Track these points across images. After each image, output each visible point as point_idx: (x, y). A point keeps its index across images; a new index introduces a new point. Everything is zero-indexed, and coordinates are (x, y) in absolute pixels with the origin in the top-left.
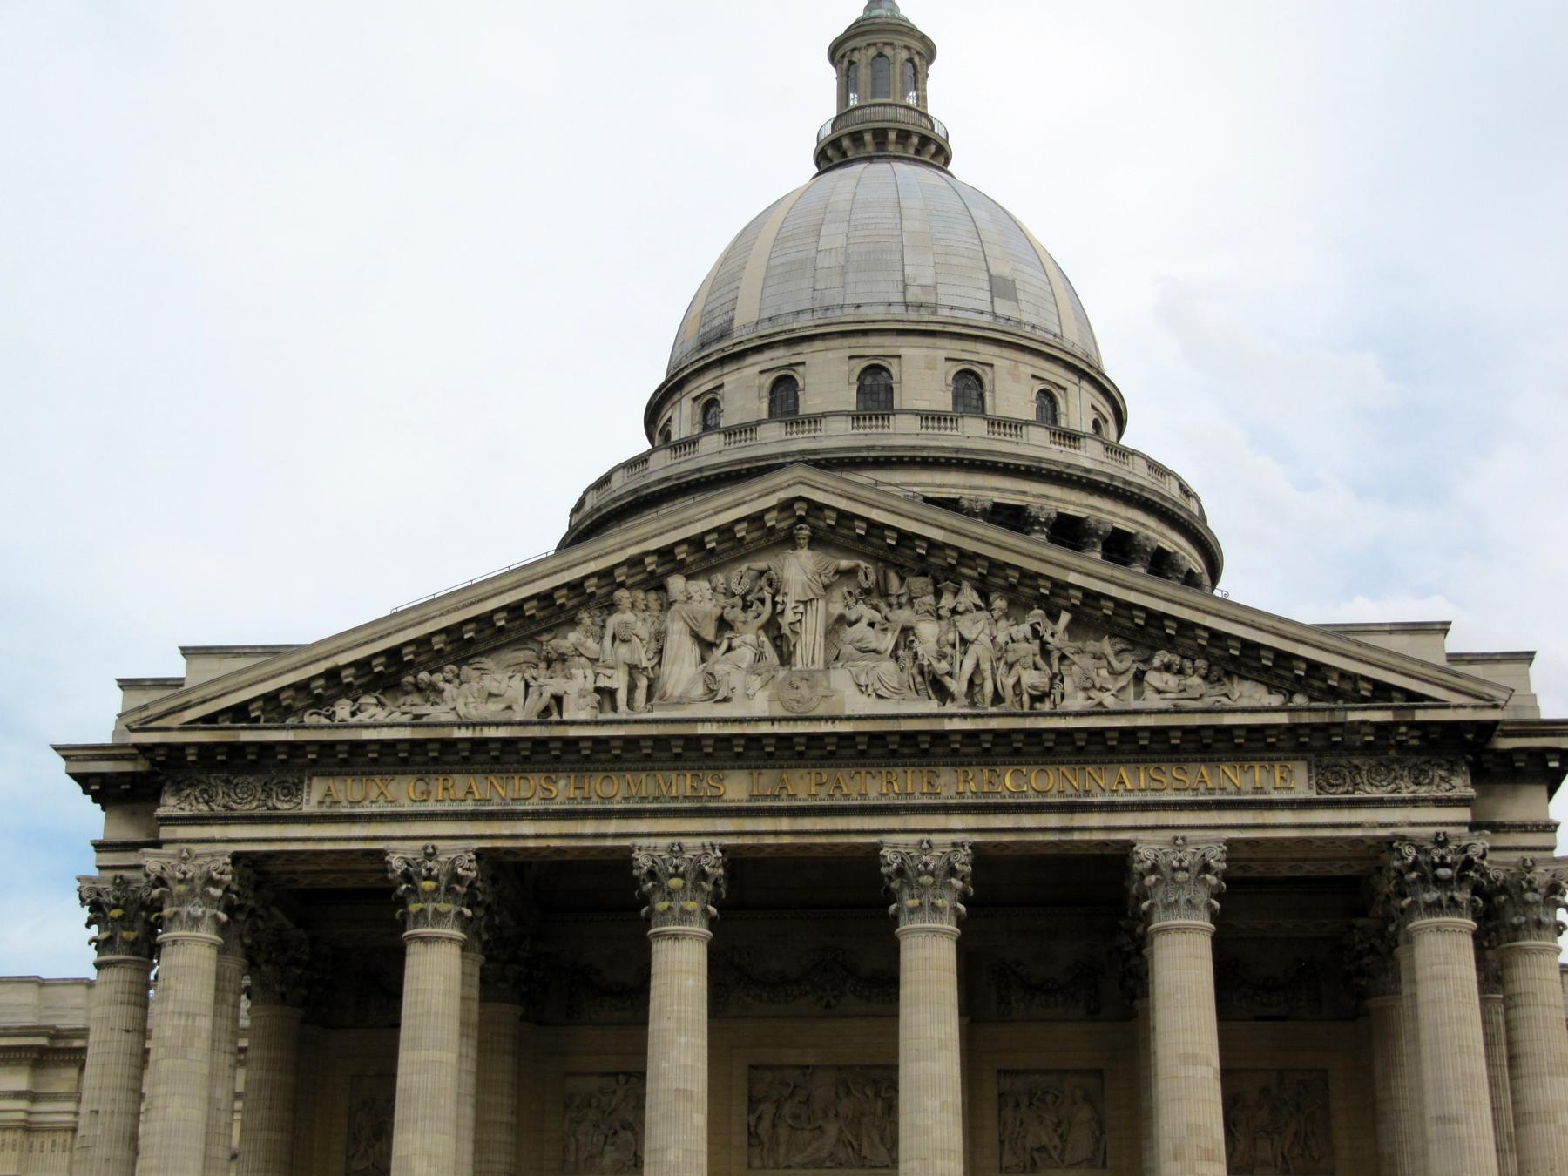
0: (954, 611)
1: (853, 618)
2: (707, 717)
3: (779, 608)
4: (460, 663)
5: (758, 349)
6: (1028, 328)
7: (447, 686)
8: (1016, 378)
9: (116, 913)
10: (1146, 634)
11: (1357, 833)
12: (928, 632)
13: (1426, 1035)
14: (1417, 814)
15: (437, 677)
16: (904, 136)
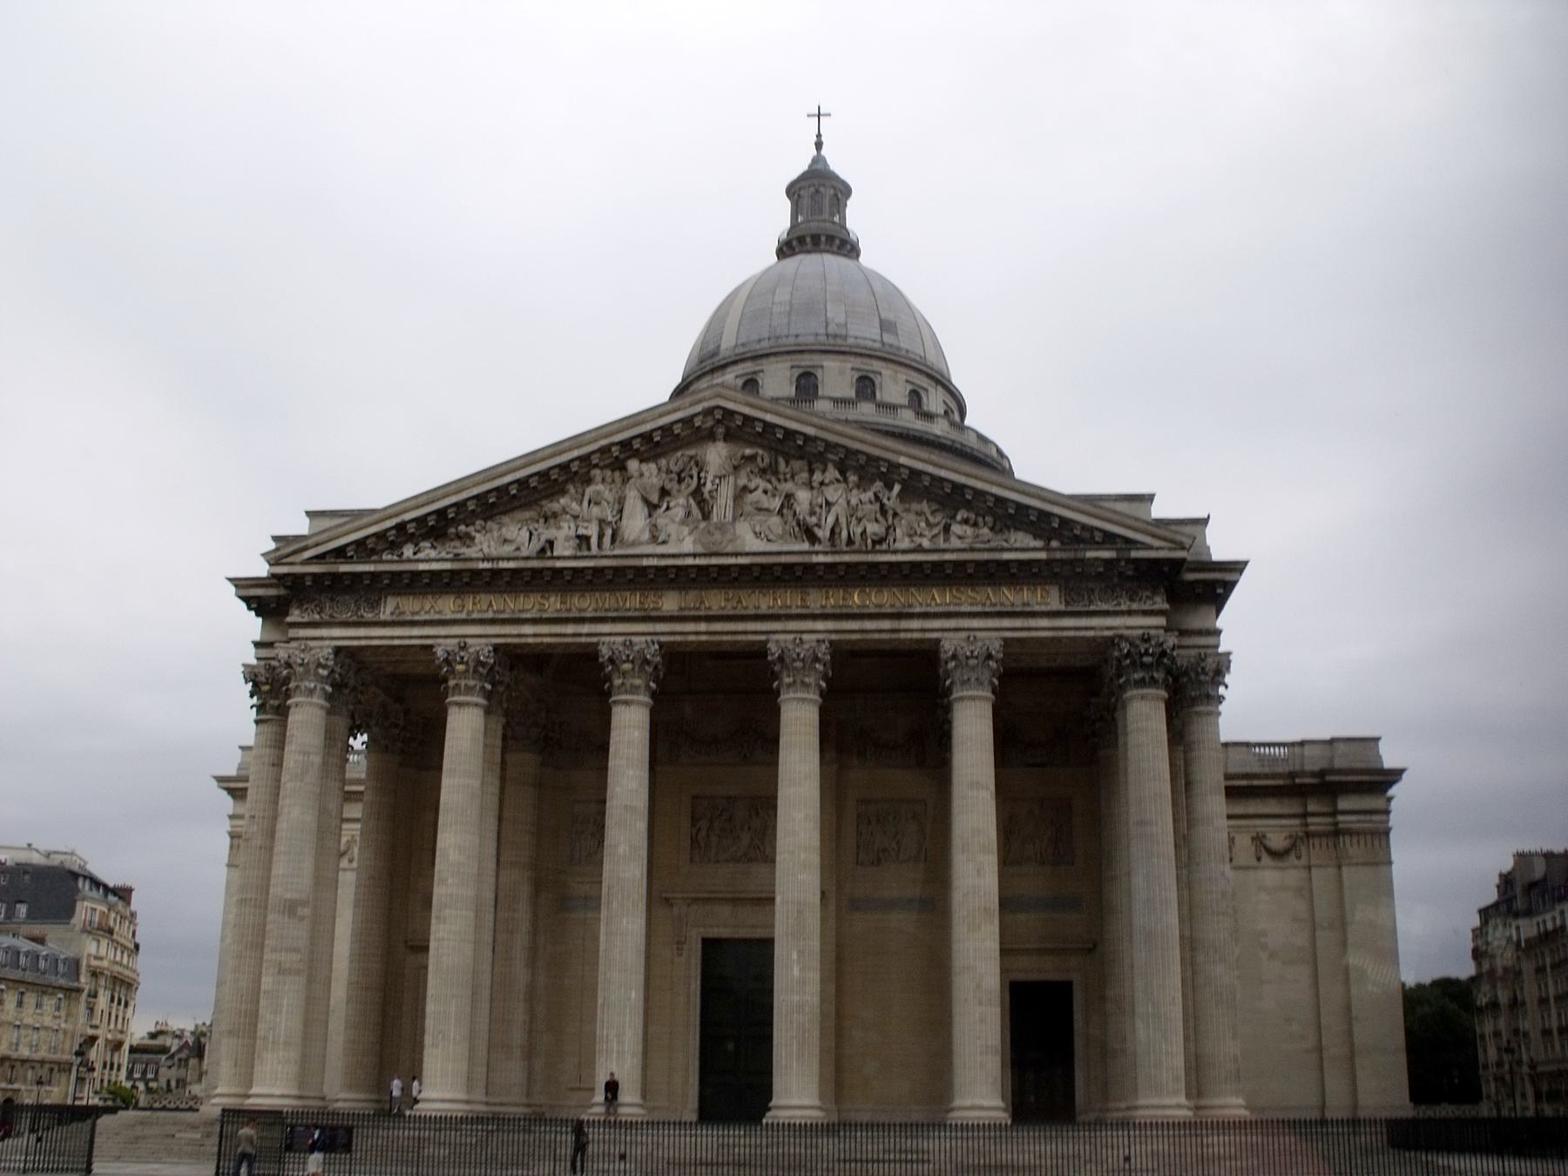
0: (822, 483)
1: (752, 486)
2: (650, 554)
4: (485, 520)
5: (735, 363)
8: (896, 381)
9: (266, 688)
10: (951, 499)
11: (1091, 633)
12: (803, 497)
13: (1132, 768)
14: (1133, 621)
15: (471, 529)
16: (830, 239)
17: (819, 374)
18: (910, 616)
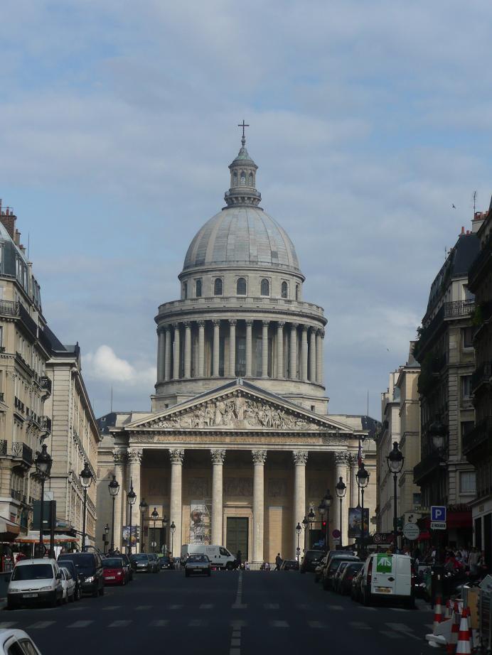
2: (223, 428)
10: (297, 415)
16: (249, 198)
18: (286, 445)
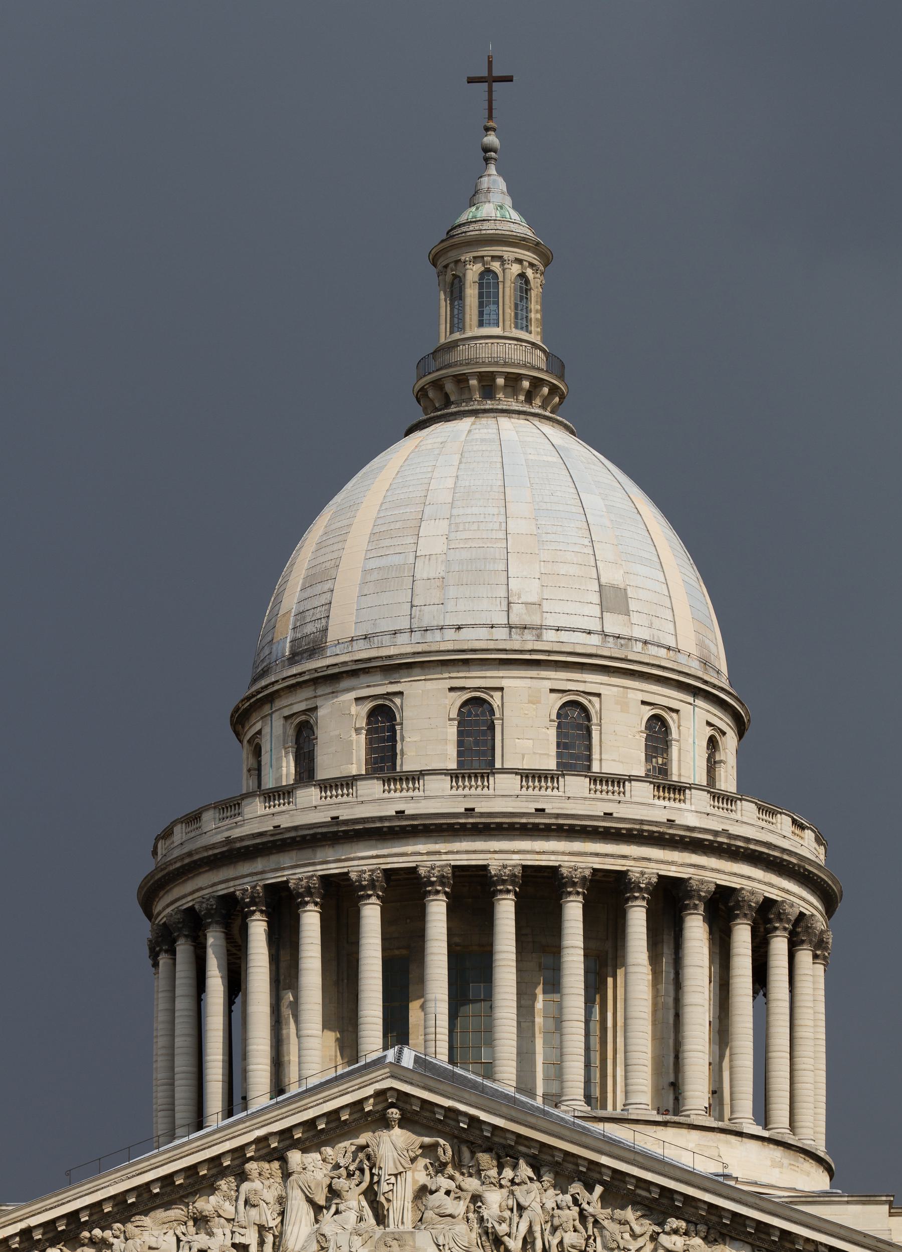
0: (512, 1182)
1: (434, 1188)
3: (376, 1179)
5: (354, 673)
6: (639, 647)
7: (115, 1241)
8: (624, 706)
12: (494, 1199)
15: (108, 1234)
17: (495, 700)
